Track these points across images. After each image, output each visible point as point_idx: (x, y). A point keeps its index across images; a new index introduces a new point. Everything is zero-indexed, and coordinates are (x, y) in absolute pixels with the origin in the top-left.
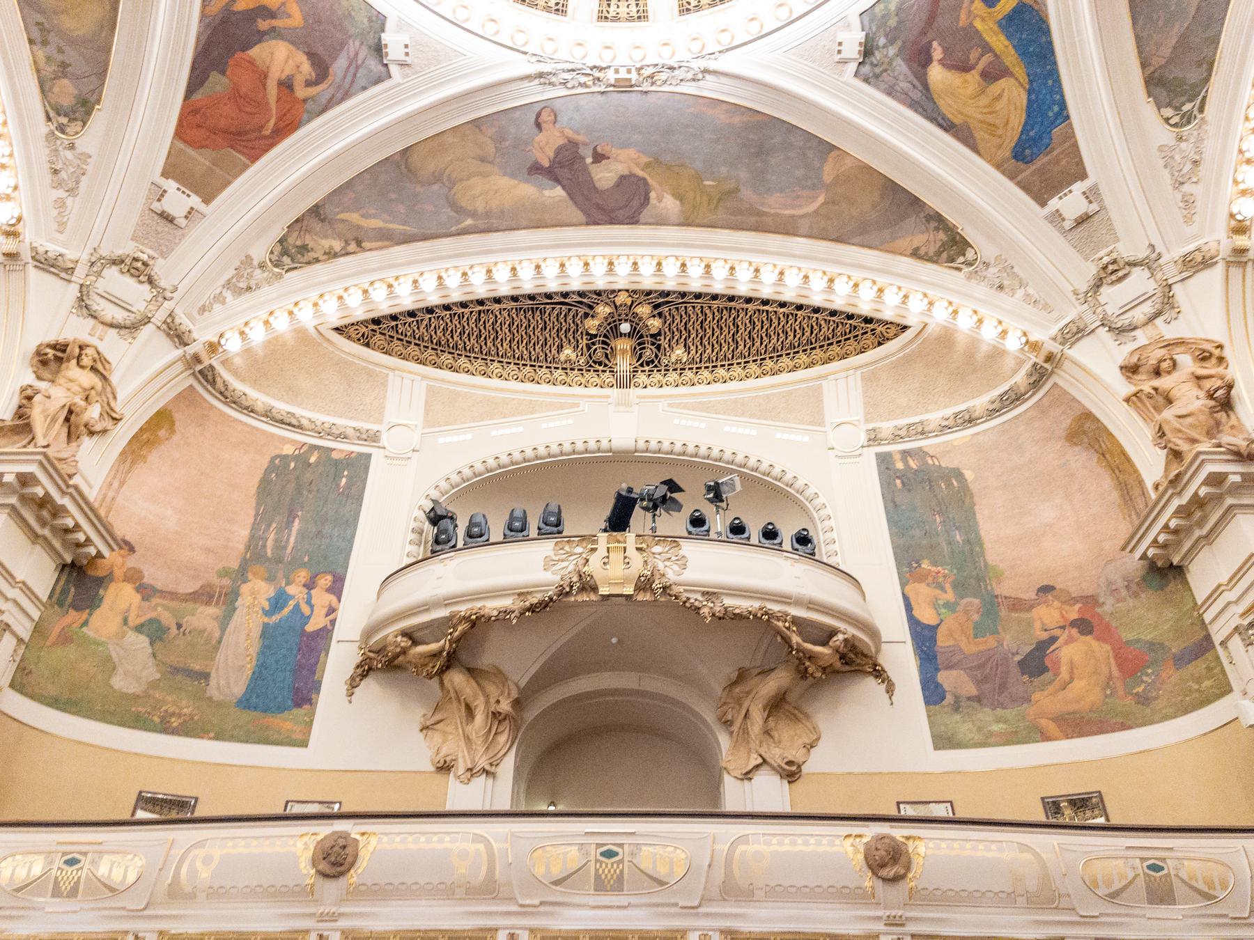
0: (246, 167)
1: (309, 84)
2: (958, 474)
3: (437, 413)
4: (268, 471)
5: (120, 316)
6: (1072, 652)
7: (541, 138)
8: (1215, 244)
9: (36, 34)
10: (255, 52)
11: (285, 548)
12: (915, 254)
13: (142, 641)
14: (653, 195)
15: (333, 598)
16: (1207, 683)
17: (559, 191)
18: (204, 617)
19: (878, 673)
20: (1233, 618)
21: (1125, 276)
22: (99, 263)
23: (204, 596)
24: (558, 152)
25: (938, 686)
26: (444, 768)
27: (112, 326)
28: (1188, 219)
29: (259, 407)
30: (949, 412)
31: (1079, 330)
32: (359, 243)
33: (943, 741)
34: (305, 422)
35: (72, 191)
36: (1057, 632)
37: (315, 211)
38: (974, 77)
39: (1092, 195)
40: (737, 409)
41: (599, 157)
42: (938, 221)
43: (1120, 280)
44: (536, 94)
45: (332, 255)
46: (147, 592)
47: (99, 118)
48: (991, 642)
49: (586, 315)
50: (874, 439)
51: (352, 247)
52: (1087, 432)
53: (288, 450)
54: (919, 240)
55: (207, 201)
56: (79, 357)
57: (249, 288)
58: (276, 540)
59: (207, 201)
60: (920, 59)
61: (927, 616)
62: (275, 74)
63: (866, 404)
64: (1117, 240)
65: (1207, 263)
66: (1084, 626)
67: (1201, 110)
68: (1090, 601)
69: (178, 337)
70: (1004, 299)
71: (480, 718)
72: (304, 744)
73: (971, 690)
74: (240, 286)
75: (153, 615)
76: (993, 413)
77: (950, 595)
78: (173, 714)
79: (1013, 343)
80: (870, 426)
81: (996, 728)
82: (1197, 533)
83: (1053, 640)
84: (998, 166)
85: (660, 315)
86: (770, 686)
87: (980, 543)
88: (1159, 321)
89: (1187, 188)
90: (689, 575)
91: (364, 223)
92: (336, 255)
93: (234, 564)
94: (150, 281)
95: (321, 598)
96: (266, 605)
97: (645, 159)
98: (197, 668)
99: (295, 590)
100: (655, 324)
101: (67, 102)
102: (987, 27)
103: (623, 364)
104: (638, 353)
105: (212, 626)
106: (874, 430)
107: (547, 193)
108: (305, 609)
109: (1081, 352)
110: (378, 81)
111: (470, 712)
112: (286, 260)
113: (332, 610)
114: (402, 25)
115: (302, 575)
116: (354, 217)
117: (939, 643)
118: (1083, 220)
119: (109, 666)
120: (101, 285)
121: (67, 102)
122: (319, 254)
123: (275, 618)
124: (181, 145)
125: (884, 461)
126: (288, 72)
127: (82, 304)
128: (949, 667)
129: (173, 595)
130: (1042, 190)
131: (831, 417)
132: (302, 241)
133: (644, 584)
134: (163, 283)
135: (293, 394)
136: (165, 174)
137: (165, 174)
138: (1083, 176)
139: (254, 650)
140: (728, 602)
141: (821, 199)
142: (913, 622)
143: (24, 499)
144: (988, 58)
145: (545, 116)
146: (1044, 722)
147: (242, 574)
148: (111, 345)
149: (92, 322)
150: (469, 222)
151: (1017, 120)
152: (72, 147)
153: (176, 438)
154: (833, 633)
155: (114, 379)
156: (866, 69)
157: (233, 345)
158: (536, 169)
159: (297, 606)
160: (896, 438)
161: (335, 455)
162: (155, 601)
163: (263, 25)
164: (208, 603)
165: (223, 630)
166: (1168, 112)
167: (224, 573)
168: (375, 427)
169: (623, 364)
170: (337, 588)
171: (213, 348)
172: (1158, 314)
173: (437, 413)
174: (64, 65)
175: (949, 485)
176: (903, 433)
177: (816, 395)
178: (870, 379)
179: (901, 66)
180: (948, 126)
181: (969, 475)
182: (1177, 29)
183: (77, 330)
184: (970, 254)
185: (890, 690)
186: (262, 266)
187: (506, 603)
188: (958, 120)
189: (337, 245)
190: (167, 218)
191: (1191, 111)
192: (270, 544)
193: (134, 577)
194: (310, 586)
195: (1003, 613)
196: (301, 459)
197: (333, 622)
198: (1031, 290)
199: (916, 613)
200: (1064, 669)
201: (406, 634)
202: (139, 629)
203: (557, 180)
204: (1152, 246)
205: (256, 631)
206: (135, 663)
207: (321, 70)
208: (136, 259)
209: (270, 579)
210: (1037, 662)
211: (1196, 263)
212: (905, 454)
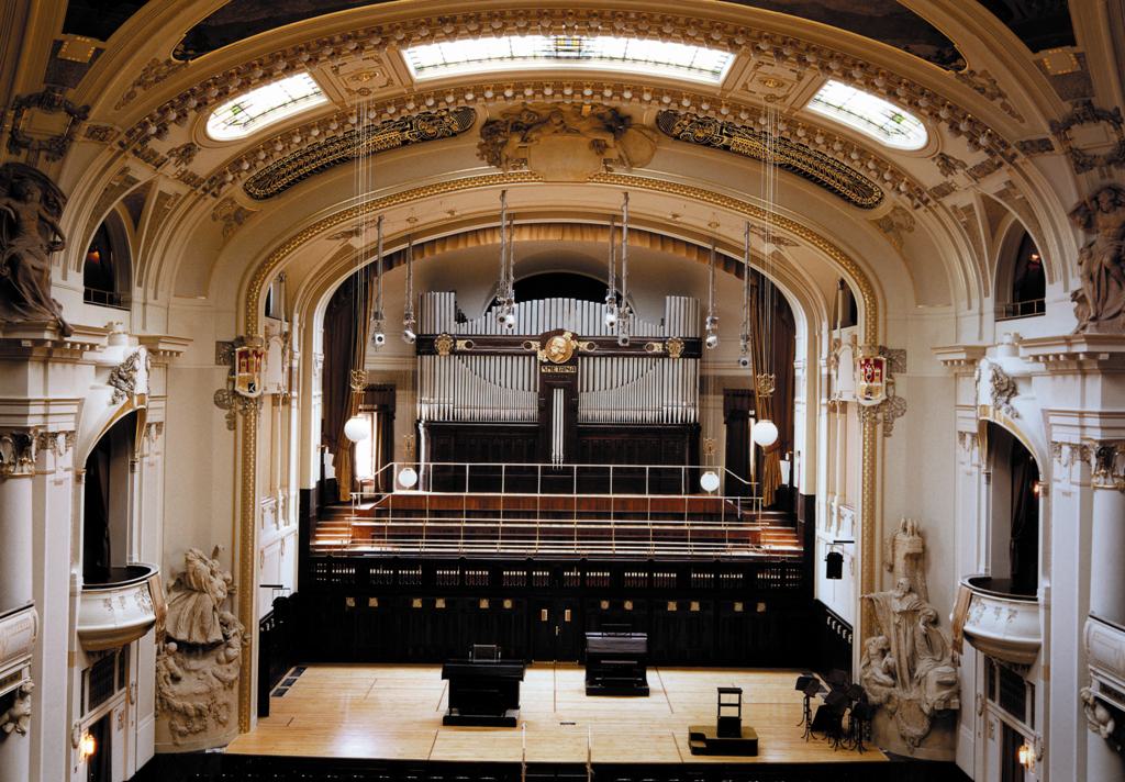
39: (98, 52)
89: (139, 90)
138: (104, 39)
172: (49, 150)
191: (190, 55)
204: (87, 109)
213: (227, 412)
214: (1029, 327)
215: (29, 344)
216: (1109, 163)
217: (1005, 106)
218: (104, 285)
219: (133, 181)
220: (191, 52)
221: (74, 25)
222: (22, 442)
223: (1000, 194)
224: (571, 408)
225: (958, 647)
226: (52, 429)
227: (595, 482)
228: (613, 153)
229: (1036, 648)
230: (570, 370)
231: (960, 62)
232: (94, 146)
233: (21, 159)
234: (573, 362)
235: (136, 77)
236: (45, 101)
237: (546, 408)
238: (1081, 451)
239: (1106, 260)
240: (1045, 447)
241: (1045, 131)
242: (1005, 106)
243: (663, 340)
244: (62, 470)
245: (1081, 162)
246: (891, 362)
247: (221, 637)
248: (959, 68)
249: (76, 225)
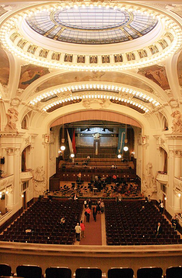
20: (5, 147)
39: (23, 91)
42: (8, 81)
65: (24, 104)
89: (29, 97)
109: (6, 104)
130: (19, 87)
138: (24, 89)
144: (32, 75)
180: (21, 76)
182: (44, 86)
211: (23, 104)
213: (44, 145)
214: (166, 132)
215: (13, 135)
216: (177, 107)
217: (161, 99)
218: (24, 126)
219: (29, 110)
221: (19, 87)
222: (12, 150)
223: (161, 112)
224: (99, 144)
225: (156, 182)
227: (103, 157)
228: (103, 105)
229: (167, 182)
230: (99, 139)
231: (154, 92)
234: (99, 138)
235: (29, 95)
236: (16, 99)
237: (95, 145)
238: (173, 151)
239: (176, 122)
240: (168, 151)
241: (167, 103)
242: (161, 99)
243: (113, 134)
244: (18, 154)
245: (172, 107)
246: (146, 137)
247: (43, 180)
248: (154, 93)
249: (20, 118)
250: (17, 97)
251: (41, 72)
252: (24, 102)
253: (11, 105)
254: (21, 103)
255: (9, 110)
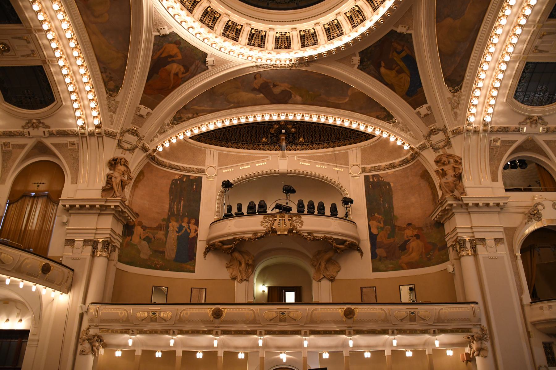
0: (164, 98)
1: (183, 73)
2: (389, 184)
3: (223, 162)
4: (172, 185)
5: (129, 146)
6: (414, 244)
7: (256, 81)
8: (461, 128)
9: (103, 70)
10: (168, 67)
11: (180, 210)
12: (377, 117)
13: (145, 243)
14: (293, 96)
15: (196, 227)
16: (445, 257)
17: (262, 95)
18: (160, 234)
19: (359, 250)
21: (437, 133)
22: (123, 133)
23: (159, 228)
24: (262, 84)
25: (376, 253)
26: (234, 279)
27: (127, 150)
28: (456, 120)
29: (167, 165)
30: (388, 163)
31: (424, 147)
32: (197, 114)
33: (375, 270)
34: (181, 168)
35: (115, 112)
36: (410, 238)
37: (184, 107)
38: (394, 73)
39: (429, 108)
40: (320, 159)
41: (275, 86)
43: (436, 134)
44: (255, 70)
45: (189, 119)
46: (144, 228)
47: (121, 91)
48: (392, 240)
49: (270, 128)
50: (364, 170)
51: (195, 115)
52: (425, 175)
53: (177, 177)
54: (378, 114)
55: (152, 110)
56: (120, 163)
57: (164, 132)
58: (177, 208)
59: (152, 110)
60: (378, 66)
61: (375, 231)
62: (173, 72)
63: (362, 159)
64: (436, 122)
66: (417, 237)
67: (461, 89)
68: (420, 229)
69: (145, 149)
70: (404, 134)
71: (243, 265)
72: (194, 272)
73: (385, 254)
74: (162, 132)
75: (147, 235)
76: (400, 165)
77: (382, 225)
78: (157, 264)
79: (406, 147)
80: (363, 166)
81: (390, 266)
82: (446, 217)
83: (409, 240)
84: (402, 97)
85: (295, 128)
86: (327, 256)
87: (393, 208)
88: (446, 148)
89: (455, 110)
90: (304, 228)
91: (199, 108)
92: (190, 118)
93: (166, 217)
94: (137, 135)
95: (193, 227)
96: (177, 230)
97: (290, 86)
98: (161, 250)
99: (183, 224)
100: (293, 130)
101: (112, 87)
102: (397, 58)
103: (283, 143)
104: (287, 139)
105: (163, 237)
106: (364, 168)
107: (258, 96)
108: (188, 230)
109: (424, 153)
110: (205, 70)
111: (240, 264)
112: (175, 122)
113: (196, 231)
114: (212, 55)
115: (186, 220)
116: (196, 107)
117: (378, 240)
118: (426, 115)
119: (139, 252)
120: (124, 139)
121: (112, 87)
122: (185, 119)
123: (180, 234)
124: (145, 95)
125: (366, 178)
126: (177, 71)
127: (119, 146)
128: (380, 248)
129: (151, 228)
131: (351, 163)
132: (181, 117)
133: (290, 231)
134: (141, 136)
135: (177, 159)
136: (140, 104)
137: (140, 104)
139: (175, 244)
140: (315, 235)
141: (347, 100)
142: (370, 233)
143: (116, 211)
145: (257, 76)
146: (403, 264)
147: (168, 220)
148: (128, 156)
149: (122, 150)
150: (232, 105)
151: (407, 85)
152: (114, 100)
153: (145, 178)
154: (346, 241)
155: (129, 167)
156: (361, 67)
157: (160, 149)
158: (254, 90)
159: (186, 230)
160: (371, 171)
161: (191, 178)
162: (147, 230)
163: (170, 60)
164: (161, 230)
165: (166, 237)
166: (451, 88)
167: (164, 220)
168: (203, 168)
169: (283, 143)
170: (197, 224)
171: (155, 150)
172: (446, 146)
173: (223, 162)
174: (111, 78)
175: (386, 187)
176: (373, 169)
177: (346, 155)
178: (363, 151)
179: (372, 67)
181: (392, 184)
183: (119, 154)
184: (394, 120)
185: (362, 254)
186: (168, 125)
187: (251, 235)
188: (389, 83)
189: (190, 116)
190: (141, 116)
192: (175, 209)
193: (140, 224)
194: (189, 223)
195: (396, 231)
196: (181, 180)
197: (197, 234)
198: (412, 133)
199: (372, 230)
200: (411, 249)
201: (221, 242)
202: (144, 240)
203: (261, 92)
204: (445, 126)
205: (175, 239)
206: (145, 251)
207: (187, 69)
208: (133, 130)
209: (177, 221)
210: (404, 247)
211: (457, 133)
212: (373, 176)
220: (456, 88)
226: (477, 236)
232: (459, 137)
233: (441, 153)
250: (432, 125)
251: (399, 48)
252: (455, 128)
253: (436, 149)
254: (450, 134)
255: (437, 162)
